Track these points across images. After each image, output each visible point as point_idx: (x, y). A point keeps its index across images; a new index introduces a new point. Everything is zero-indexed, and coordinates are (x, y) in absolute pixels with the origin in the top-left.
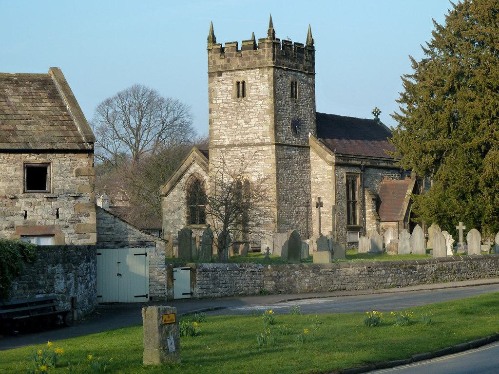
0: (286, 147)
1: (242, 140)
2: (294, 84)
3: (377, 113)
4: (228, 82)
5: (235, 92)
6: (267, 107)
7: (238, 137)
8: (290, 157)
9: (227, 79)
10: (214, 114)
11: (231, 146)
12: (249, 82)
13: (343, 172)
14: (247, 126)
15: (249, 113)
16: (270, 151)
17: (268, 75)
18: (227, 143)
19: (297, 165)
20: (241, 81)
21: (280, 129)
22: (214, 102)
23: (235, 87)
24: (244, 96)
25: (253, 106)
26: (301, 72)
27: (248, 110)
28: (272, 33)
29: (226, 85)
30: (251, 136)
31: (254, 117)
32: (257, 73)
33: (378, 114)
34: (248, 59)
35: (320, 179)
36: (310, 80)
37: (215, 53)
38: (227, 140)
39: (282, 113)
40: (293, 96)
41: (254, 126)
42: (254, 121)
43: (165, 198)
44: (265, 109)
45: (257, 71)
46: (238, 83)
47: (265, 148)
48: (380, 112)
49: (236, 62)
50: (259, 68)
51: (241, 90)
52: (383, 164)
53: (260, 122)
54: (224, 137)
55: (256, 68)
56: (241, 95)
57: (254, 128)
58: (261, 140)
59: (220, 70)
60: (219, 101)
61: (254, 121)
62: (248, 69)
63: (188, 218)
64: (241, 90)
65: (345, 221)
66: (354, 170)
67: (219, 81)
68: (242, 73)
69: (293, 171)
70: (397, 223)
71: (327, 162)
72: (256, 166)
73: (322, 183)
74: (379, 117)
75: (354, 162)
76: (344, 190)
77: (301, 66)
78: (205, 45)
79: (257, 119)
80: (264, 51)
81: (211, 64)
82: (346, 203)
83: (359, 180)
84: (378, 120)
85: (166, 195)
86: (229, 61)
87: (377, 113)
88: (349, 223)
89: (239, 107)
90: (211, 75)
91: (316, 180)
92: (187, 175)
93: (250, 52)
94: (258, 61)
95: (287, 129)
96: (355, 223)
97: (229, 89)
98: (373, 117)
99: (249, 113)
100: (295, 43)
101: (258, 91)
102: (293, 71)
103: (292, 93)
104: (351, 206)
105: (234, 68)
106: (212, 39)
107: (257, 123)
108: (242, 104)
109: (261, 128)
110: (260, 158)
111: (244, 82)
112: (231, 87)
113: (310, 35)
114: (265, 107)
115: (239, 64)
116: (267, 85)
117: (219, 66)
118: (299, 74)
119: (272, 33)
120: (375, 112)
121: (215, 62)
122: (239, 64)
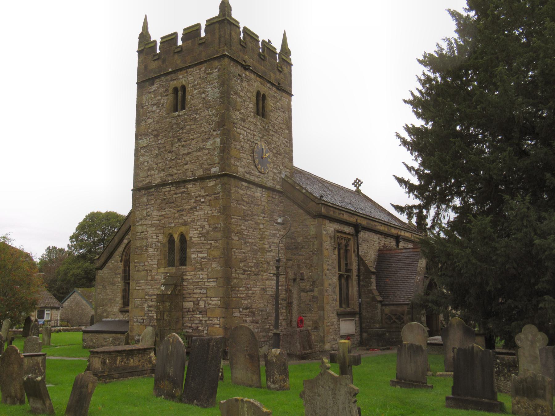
0: (246, 184)
1: (176, 173)
3: (358, 183)
11: (164, 184)
16: (219, 188)
19: (263, 215)
21: (234, 152)
26: (272, 84)
27: (188, 127)
30: (189, 166)
32: (203, 69)
33: (360, 185)
38: (156, 176)
43: (100, 271)
44: (213, 121)
47: (211, 183)
48: (362, 183)
50: (205, 62)
54: (153, 172)
55: (201, 63)
66: (347, 229)
71: (309, 213)
72: (196, 213)
74: (360, 188)
76: (335, 256)
82: (337, 276)
83: (352, 243)
86: (164, 61)
87: (358, 183)
88: (341, 306)
94: (204, 54)
98: (354, 189)
101: (203, 96)
104: (343, 281)
105: (170, 70)
106: (144, 37)
110: (203, 200)
111: (184, 88)
112: (167, 101)
115: (179, 62)
118: (269, 85)
120: (355, 184)
122: (179, 62)
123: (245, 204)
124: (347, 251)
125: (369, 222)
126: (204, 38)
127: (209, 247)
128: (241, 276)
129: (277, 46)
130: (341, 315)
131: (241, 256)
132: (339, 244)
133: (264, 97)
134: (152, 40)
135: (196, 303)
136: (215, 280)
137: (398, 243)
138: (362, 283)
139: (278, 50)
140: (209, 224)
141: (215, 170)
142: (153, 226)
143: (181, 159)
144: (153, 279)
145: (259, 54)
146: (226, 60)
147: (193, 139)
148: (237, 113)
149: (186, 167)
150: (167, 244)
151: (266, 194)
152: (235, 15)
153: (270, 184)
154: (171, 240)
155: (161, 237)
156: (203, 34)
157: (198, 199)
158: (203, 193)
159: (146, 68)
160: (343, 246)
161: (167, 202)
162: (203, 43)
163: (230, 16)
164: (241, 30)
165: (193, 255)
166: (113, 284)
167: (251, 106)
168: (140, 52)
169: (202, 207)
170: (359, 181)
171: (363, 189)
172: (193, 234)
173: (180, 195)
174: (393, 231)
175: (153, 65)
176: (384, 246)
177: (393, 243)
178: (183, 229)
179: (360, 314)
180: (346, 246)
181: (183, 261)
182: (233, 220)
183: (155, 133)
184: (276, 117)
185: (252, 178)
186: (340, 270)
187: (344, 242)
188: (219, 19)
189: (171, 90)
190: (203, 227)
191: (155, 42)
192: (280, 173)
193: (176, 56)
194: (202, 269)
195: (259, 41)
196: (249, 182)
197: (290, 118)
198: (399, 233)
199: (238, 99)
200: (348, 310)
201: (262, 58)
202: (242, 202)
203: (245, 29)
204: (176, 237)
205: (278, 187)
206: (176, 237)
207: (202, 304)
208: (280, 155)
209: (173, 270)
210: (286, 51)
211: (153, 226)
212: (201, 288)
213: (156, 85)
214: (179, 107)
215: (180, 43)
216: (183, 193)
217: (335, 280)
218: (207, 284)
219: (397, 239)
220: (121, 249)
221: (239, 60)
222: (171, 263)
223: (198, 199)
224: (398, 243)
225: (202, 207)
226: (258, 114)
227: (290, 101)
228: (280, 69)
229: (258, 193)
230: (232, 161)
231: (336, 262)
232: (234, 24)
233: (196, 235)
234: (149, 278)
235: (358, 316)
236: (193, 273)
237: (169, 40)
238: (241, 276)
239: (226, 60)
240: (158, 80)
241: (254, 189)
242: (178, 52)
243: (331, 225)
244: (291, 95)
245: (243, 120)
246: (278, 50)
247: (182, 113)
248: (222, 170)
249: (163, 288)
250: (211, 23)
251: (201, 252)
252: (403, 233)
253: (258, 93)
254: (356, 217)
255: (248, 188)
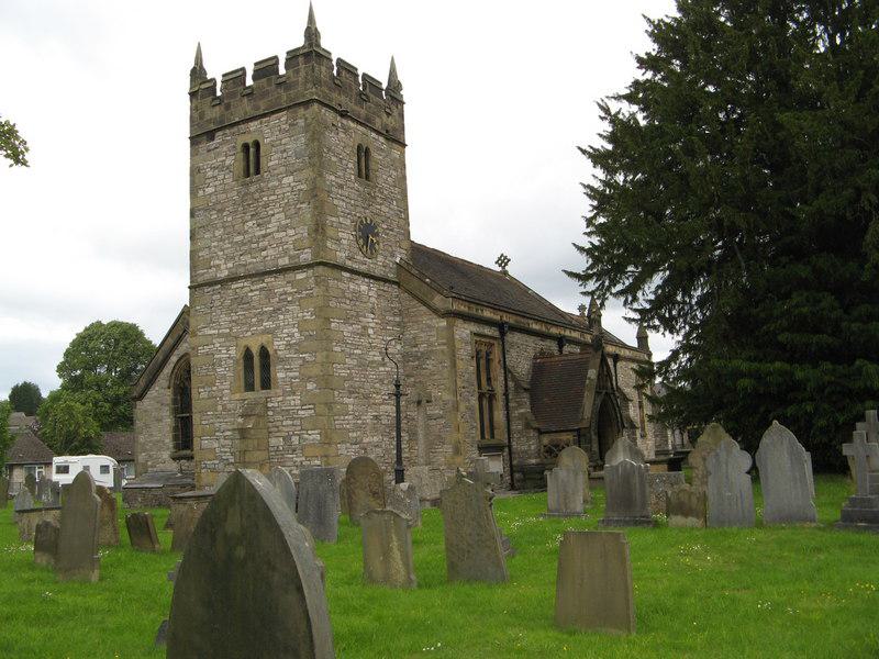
0: (347, 275)
1: (250, 263)
2: (363, 153)
3: (503, 261)
4: (225, 149)
5: (240, 165)
6: (304, 187)
7: (247, 259)
8: (357, 297)
9: (224, 142)
10: (200, 219)
11: (233, 279)
12: (265, 142)
13: (464, 331)
14: (263, 232)
15: (266, 206)
17: (306, 119)
18: (224, 274)
19: (372, 316)
20: (250, 141)
21: (330, 232)
22: (201, 192)
23: (241, 156)
24: (258, 172)
25: (276, 187)
26: (378, 133)
28: (312, 34)
29: (226, 152)
30: (270, 252)
31: (276, 211)
33: (506, 264)
34: (264, 94)
35: (423, 348)
36: (396, 154)
37: (202, 97)
38: (223, 267)
39: (336, 202)
40: (364, 172)
41: (278, 231)
42: (279, 218)
43: (138, 403)
45: (283, 116)
46: (246, 147)
47: (300, 276)
49: (245, 107)
51: (252, 158)
52: (535, 327)
53: (288, 221)
54: (217, 262)
56: (252, 170)
57: (277, 235)
58: (291, 258)
59: (212, 127)
60: (210, 190)
61: (279, 218)
62: (264, 115)
63: (175, 438)
64: (252, 158)
65: (476, 433)
66: (487, 331)
67: (209, 151)
68: (253, 125)
69: (365, 328)
70: (575, 434)
71: (435, 311)
72: (281, 317)
73: (426, 356)
75: (487, 314)
76: (472, 369)
77: (378, 120)
78: (185, 84)
79: (282, 215)
80: (297, 72)
81: (196, 119)
83: (497, 351)
84: (506, 273)
85: (141, 397)
86: (228, 107)
88: (483, 436)
89: (246, 194)
90: (194, 140)
91: (414, 349)
92: (174, 359)
93: (269, 81)
95: (347, 236)
96: (493, 436)
97: (227, 163)
98: (499, 269)
99: (266, 206)
100: (364, 75)
102: (361, 124)
103: (360, 170)
104: (485, 403)
105: (237, 120)
106: (198, 73)
107: (283, 222)
108: (253, 189)
109: (291, 232)
111: (257, 145)
112: (233, 160)
113: (393, 73)
114: (298, 187)
115: (248, 109)
116: (303, 140)
117: (209, 121)
118: (373, 135)
119: (312, 34)
121: (201, 116)
122: (248, 109)
123: (348, 302)
124: (488, 361)
125: (519, 318)
126: (284, 76)
127: (300, 362)
128: (346, 400)
129: (383, 79)
130: (483, 449)
131: (344, 373)
132: (478, 353)
133: (367, 151)
134: (209, 77)
135: (287, 439)
136: (311, 406)
137: (561, 347)
138: (511, 405)
139: (384, 86)
140: (300, 332)
141: (306, 256)
142: (219, 336)
143: (257, 242)
144: (224, 409)
145: (361, 94)
146: (316, 105)
147: (273, 215)
148: (333, 178)
149: (264, 253)
150: (242, 361)
151: (375, 286)
152: (325, 43)
153: (378, 272)
154: (248, 356)
155: (233, 352)
156: (282, 71)
157: (282, 297)
158: (289, 289)
159: (201, 116)
160: (483, 354)
161: (241, 301)
162: (283, 84)
163: (319, 46)
164: (334, 63)
165: (279, 374)
166: (159, 420)
167: (350, 165)
168: (193, 95)
169: (290, 308)
170: (506, 258)
171: (512, 270)
172: (278, 346)
173: (257, 293)
174: (554, 331)
175: (215, 113)
176: (542, 353)
177: (554, 347)
178: (263, 339)
179: (510, 447)
180: (488, 354)
181: (266, 383)
182: (333, 325)
183: (219, 207)
184: (383, 177)
185: (356, 266)
186: (480, 387)
187: (484, 348)
188: (306, 50)
189: (239, 148)
190: (292, 336)
191: (213, 80)
192: (393, 256)
193: (245, 99)
194: (294, 394)
195: (358, 76)
196: (352, 271)
197: (404, 178)
198: (562, 332)
199: (334, 159)
200: (493, 442)
201: (362, 98)
202: (344, 300)
203: (339, 61)
204: (255, 350)
205: (391, 276)
206: (255, 350)
207: (295, 440)
208: (392, 230)
209: (250, 395)
210: (395, 85)
211: (219, 336)
212: (293, 419)
213: (217, 141)
214: (252, 170)
215: (249, 82)
216: (261, 289)
217: (474, 401)
218: (303, 412)
219: (561, 341)
220: (167, 370)
221: (333, 104)
222: (249, 387)
223: (282, 297)
224: (561, 347)
225: (290, 308)
226: (360, 175)
227: (403, 154)
228: (387, 110)
229: (363, 286)
230: (329, 244)
231: (474, 376)
232: (323, 57)
233: (282, 347)
234: (220, 408)
235: (507, 450)
236: (280, 399)
237: (235, 78)
238: (346, 400)
239: (316, 105)
240: (220, 133)
241: (360, 280)
242: (248, 95)
243: (466, 326)
244: (404, 145)
245: (341, 187)
246: (384, 86)
247: (255, 178)
248: (316, 254)
249: (240, 420)
250: (293, 56)
251: (290, 370)
252: (567, 333)
253: (359, 147)
254: (501, 313)
255: (351, 280)
